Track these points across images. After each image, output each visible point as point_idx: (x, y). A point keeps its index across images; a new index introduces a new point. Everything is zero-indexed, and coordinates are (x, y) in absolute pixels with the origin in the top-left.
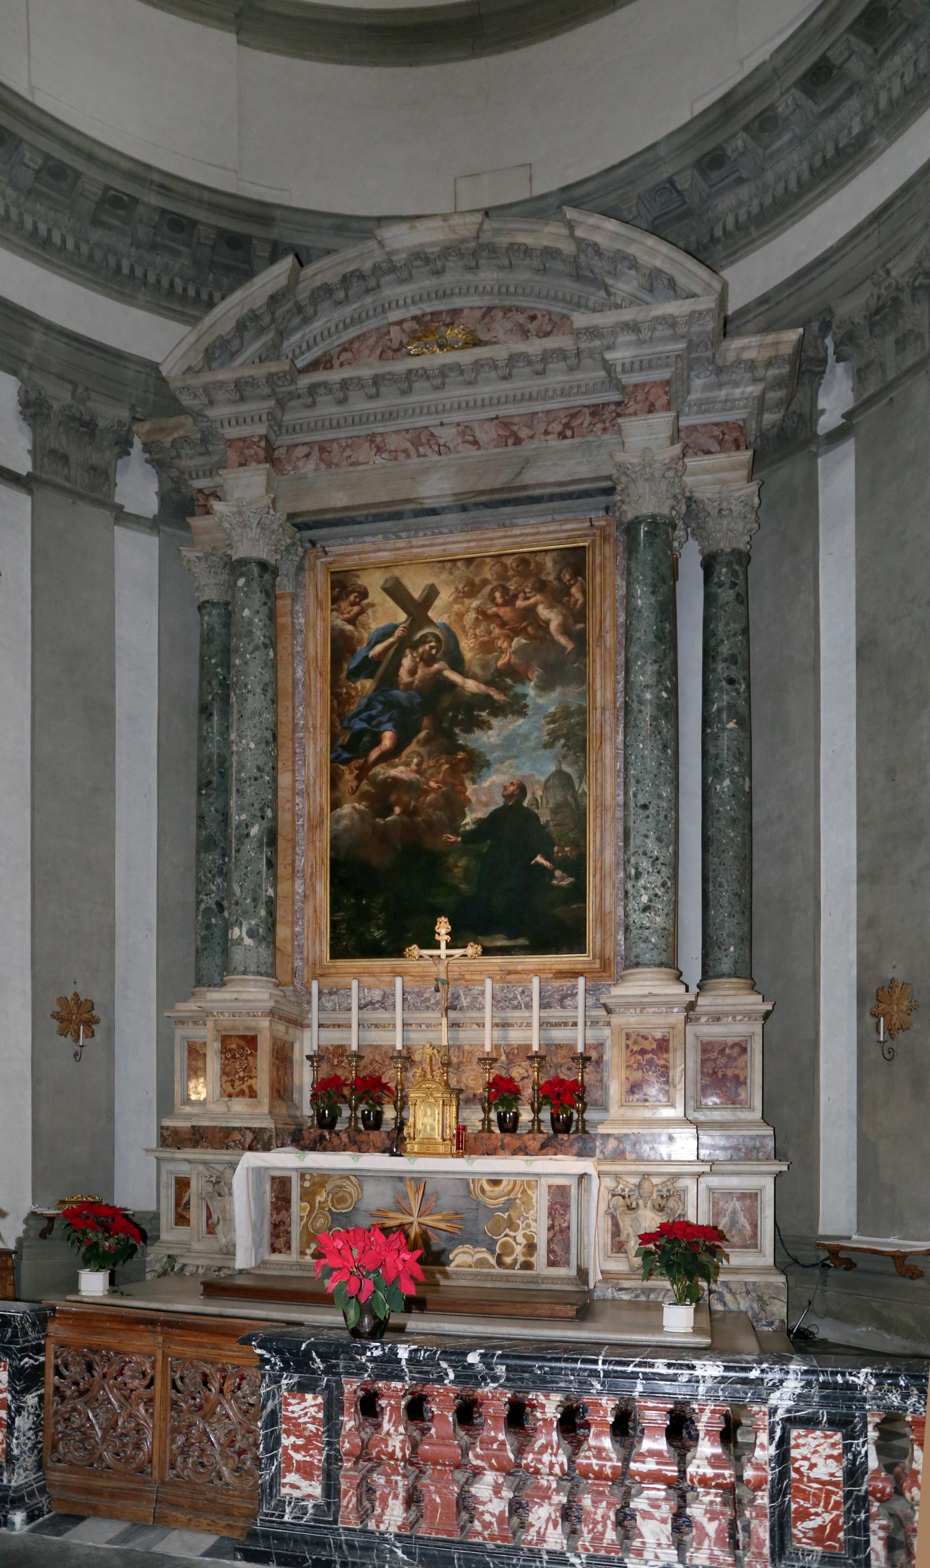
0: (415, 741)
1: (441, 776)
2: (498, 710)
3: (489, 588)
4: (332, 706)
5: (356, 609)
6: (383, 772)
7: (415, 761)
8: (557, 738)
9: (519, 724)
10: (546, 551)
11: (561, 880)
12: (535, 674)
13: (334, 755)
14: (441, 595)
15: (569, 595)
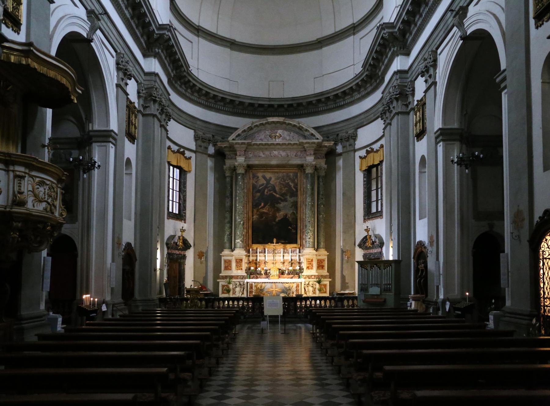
2: (282, 201)
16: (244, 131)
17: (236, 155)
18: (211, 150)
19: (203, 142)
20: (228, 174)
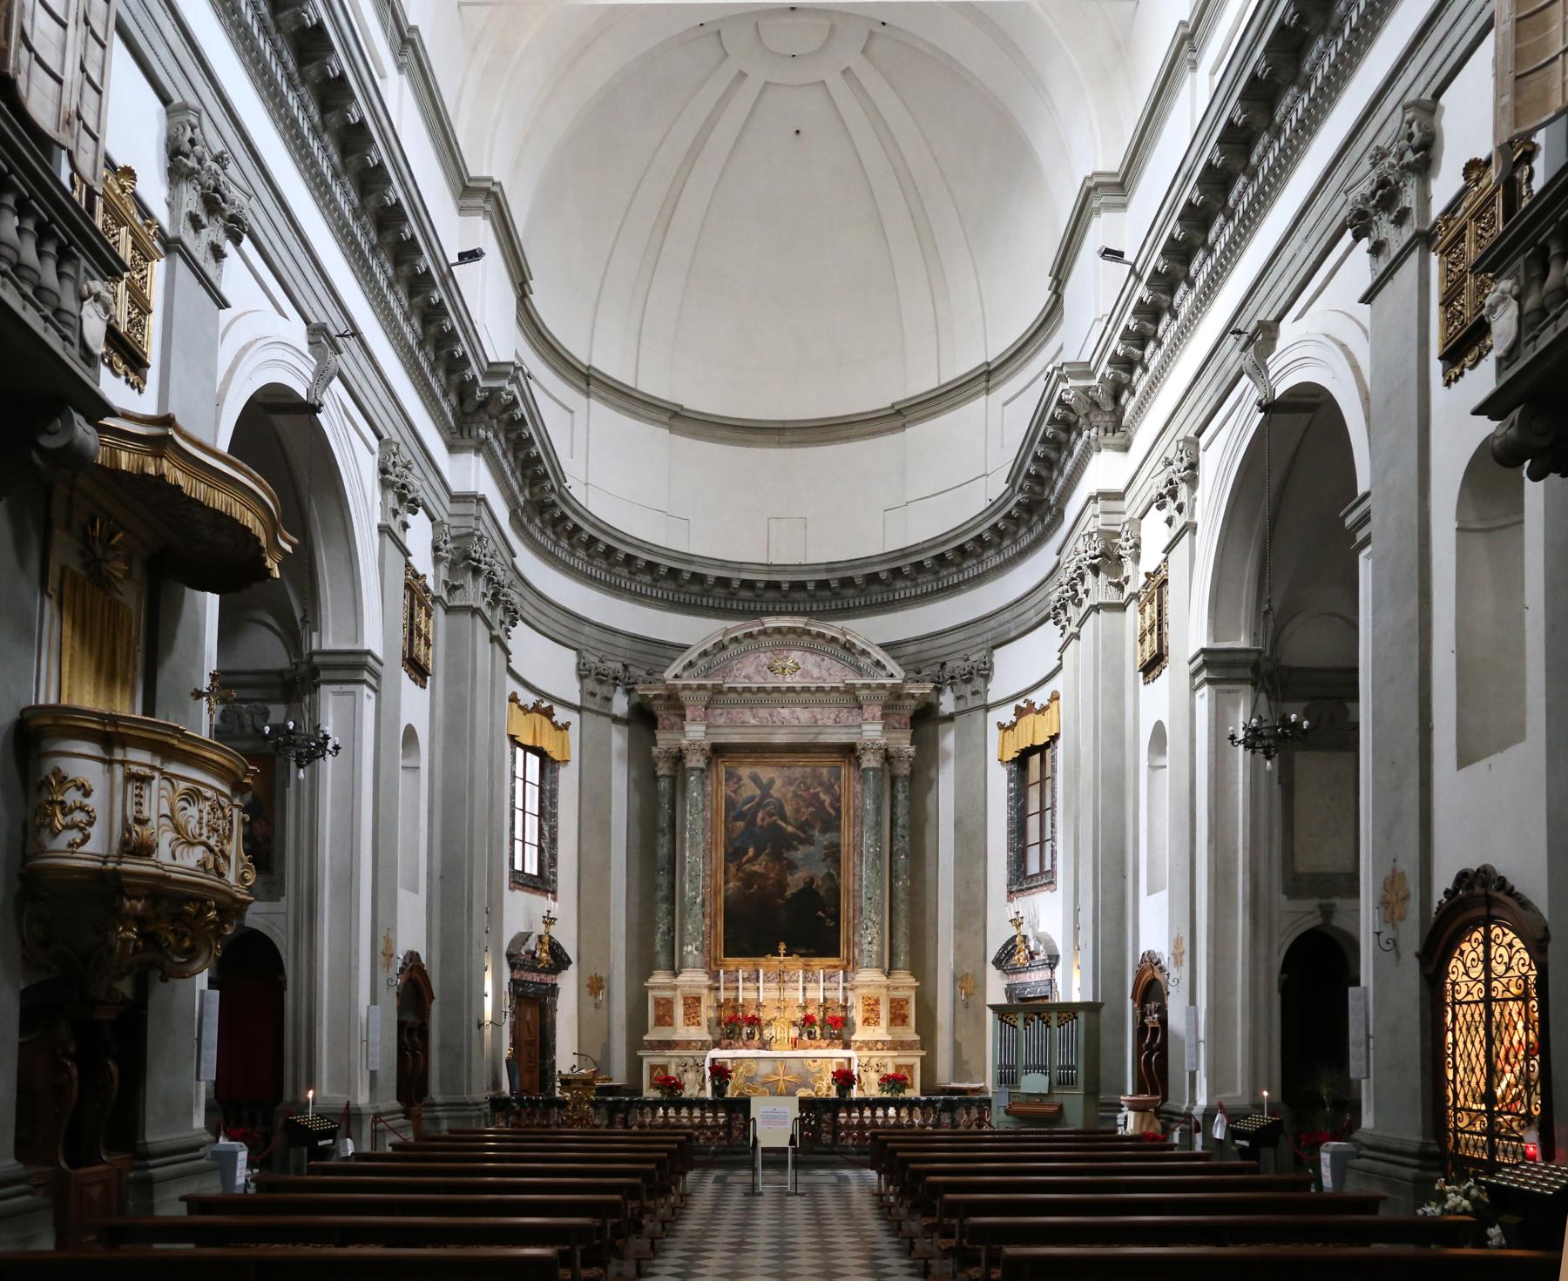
2: (801, 841)
6: (748, 867)
16: (705, 653)
17: (683, 717)
18: (620, 705)
19: (601, 682)
20: (663, 769)
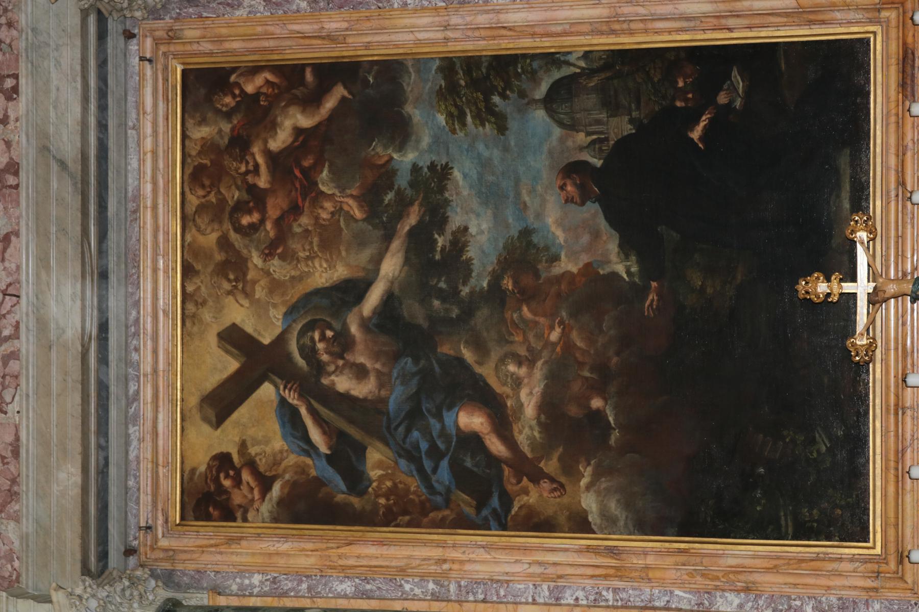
0: (478, 370)
1: (542, 320)
2: (436, 216)
3: (233, 236)
4: (409, 525)
5: (246, 476)
6: (527, 432)
7: (512, 368)
8: (491, 109)
9: (461, 178)
10: (184, 136)
11: (735, 90)
12: (380, 151)
13: (492, 523)
14: (238, 321)
15: (257, 95)
